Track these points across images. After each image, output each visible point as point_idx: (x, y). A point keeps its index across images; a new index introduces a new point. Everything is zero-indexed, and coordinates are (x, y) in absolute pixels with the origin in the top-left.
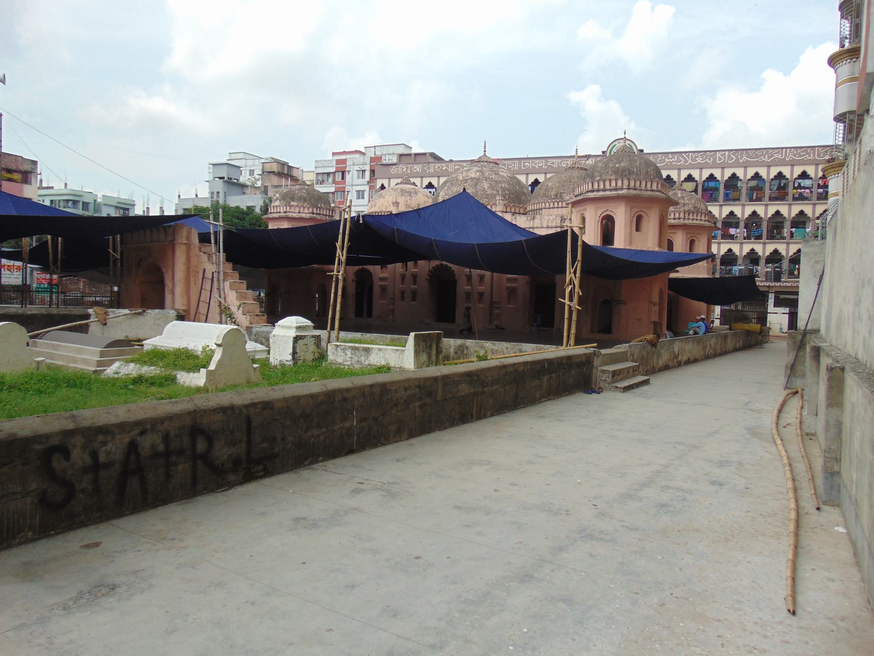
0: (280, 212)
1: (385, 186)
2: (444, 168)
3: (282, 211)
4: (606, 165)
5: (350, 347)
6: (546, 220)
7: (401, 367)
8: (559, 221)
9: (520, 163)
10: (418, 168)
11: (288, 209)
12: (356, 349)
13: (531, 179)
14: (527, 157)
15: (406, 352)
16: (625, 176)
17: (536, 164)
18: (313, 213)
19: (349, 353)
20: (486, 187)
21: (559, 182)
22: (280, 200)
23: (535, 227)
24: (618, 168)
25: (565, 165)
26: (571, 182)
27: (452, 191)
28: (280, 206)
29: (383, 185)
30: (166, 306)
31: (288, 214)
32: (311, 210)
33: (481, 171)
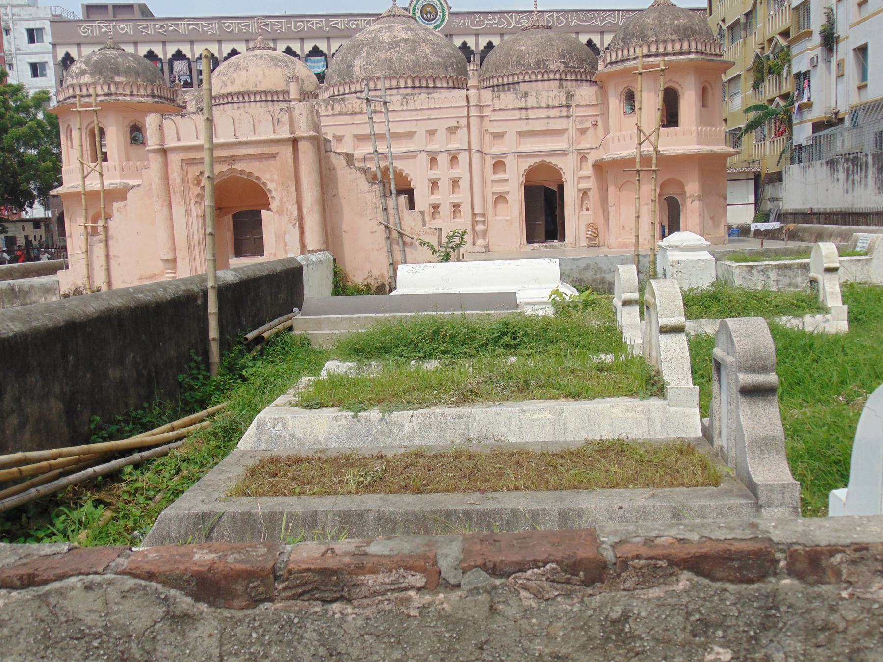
0: (125, 95)
2: (171, 29)
4: (660, 22)
5: (775, 266)
7: (866, 283)
8: (564, 98)
9: (289, 23)
10: (126, 28)
11: (113, 89)
13: (483, 42)
14: (284, 14)
15: (875, 261)
16: (689, 36)
17: (312, 24)
18: (153, 96)
19: (773, 275)
20: (428, 51)
22: (92, 75)
23: (529, 106)
24: (678, 25)
26: (552, 45)
27: (378, 58)
28: (94, 84)
29: (67, 55)
30: (682, 225)
31: (114, 97)
32: (149, 91)
33: (412, 30)
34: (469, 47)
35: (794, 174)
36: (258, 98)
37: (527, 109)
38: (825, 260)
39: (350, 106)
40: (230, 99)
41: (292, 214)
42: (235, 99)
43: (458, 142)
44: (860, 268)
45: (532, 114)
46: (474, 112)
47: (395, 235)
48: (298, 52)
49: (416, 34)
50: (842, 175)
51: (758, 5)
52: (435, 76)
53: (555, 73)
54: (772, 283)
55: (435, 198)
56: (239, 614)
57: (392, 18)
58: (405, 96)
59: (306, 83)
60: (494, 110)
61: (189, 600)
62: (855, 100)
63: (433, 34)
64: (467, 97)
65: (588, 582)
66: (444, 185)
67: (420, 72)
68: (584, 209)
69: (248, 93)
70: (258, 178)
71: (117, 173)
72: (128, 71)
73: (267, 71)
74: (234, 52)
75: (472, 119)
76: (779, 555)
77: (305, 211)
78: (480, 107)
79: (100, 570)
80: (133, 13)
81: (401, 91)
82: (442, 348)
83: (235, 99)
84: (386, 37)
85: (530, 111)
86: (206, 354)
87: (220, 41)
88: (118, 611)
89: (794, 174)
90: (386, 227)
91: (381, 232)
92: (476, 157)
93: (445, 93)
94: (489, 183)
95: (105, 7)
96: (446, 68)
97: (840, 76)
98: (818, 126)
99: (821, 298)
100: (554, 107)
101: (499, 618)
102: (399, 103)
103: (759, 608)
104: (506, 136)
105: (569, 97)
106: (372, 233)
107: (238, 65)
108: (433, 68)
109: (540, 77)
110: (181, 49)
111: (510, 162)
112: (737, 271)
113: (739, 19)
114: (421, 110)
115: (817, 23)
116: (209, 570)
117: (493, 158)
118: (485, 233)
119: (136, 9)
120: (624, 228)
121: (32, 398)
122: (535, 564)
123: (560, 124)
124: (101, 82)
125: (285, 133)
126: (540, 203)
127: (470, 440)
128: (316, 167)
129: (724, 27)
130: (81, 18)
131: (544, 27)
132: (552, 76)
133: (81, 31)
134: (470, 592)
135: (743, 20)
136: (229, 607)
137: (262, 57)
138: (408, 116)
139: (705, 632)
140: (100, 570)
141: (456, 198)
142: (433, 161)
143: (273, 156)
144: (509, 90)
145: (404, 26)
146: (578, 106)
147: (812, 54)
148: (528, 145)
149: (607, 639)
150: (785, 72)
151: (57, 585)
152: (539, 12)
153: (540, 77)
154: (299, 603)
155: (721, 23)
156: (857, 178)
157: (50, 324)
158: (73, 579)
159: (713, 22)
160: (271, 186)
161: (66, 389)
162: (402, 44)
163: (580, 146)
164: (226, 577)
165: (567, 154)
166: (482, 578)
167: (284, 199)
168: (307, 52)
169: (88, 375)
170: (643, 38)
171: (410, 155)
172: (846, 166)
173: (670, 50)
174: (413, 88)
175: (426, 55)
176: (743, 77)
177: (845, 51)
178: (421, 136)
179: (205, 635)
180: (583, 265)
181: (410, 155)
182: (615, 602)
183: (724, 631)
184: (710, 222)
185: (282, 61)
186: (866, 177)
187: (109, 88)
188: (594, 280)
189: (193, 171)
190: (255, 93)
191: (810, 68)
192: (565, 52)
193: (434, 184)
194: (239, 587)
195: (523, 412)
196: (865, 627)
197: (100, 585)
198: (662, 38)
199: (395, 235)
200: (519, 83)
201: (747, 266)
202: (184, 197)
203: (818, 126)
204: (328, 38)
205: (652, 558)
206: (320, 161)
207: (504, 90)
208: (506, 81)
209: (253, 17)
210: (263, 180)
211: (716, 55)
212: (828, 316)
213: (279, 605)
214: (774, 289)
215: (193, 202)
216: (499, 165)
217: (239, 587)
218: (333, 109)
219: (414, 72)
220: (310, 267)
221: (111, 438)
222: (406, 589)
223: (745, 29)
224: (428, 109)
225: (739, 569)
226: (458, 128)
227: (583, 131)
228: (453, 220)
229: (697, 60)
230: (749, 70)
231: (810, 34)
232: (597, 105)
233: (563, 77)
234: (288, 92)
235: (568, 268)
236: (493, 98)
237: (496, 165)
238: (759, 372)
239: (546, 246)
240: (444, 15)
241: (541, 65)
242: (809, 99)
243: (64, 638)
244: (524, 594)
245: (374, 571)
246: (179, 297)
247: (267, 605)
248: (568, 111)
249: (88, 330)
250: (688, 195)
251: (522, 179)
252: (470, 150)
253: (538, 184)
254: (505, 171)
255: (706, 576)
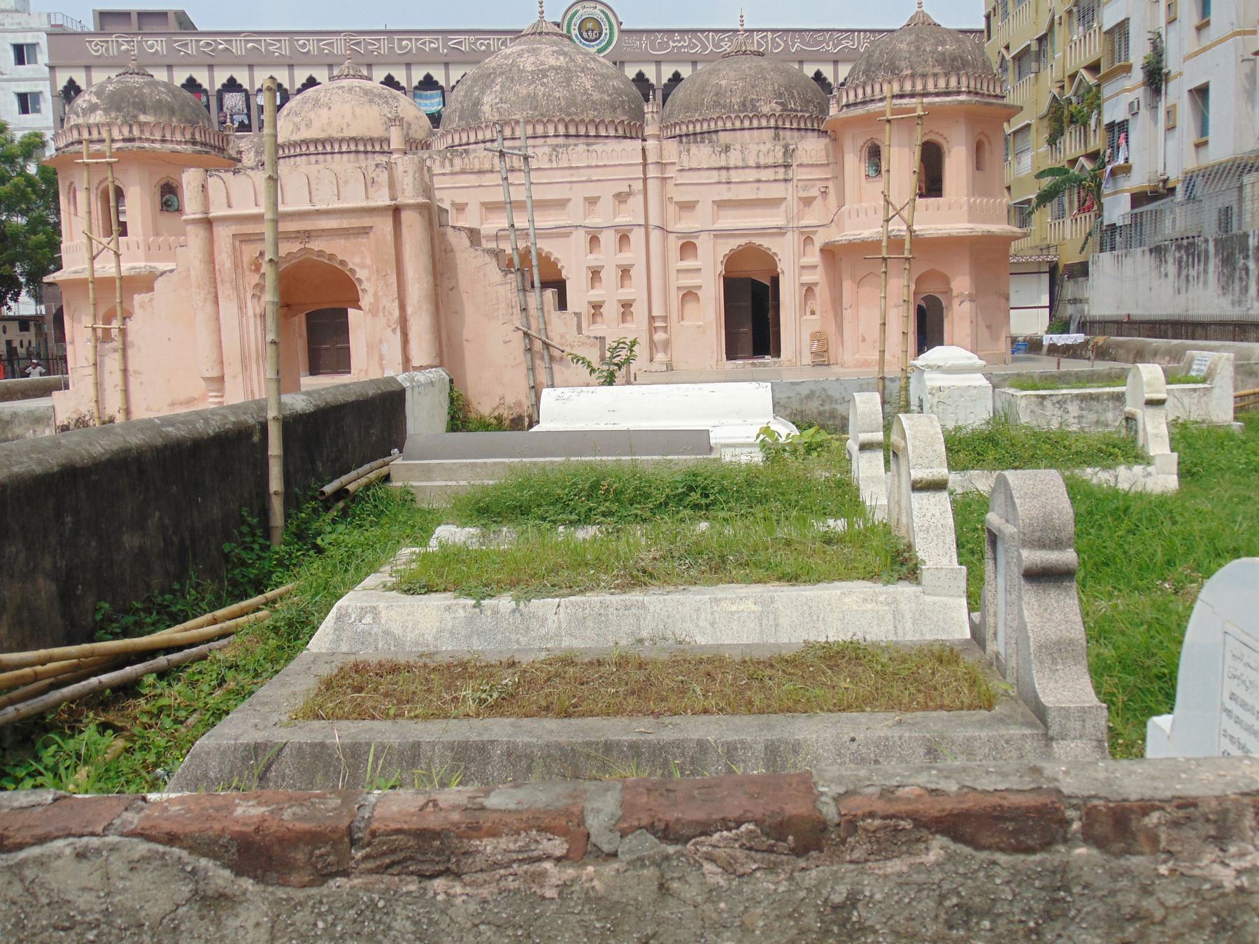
1: (78, 83)
2: (221, 47)
3: (116, 135)
4: (918, 48)
5: (1077, 395)
6: (755, 153)
7: (1203, 422)
8: (781, 154)
9: (391, 41)
10: (156, 45)
11: (136, 132)
12: (1092, 397)
13: (667, 72)
14: (382, 28)
15: (1217, 391)
16: (959, 69)
18: (194, 143)
19: (1073, 408)
20: (588, 85)
21: (744, 79)
22: (106, 111)
23: (732, 164)
25: (483, 48)
26: (765, 79)
27: (516, 94)
28: (109, 125)
29: (71, 82)
30: (946, 336)
31: (137, 144)
32: (188, 137)
33: (565, 54)
34: (647, 80)
35: (1104, 265)
36: (344, 148)
37: (728, 169)
38: (1145, 389)
39: (476, 161)
40: (304, 148)
41: (391, 314)
42: (312, 149)
43: (629, 215)
44: (1195, 401)
45: (735, 176)
46: (653, 172)
47: (538, 345)
48: (403, 83)
49: (572, 60)
50: (1172, 268)
51: (1056, 26)
52: (597, 120)
53: (768, 118)
54: (1072, 420)
55: (596, 294)
56: (300, 894)
57: (538, 37)
58: (555, 148)
59: (413, 126)
60: (682, 170)
61: (227, 873)
62: (1191, 162)
63: (595, 60)
64: (644, 150)
65: (801, 851)
66: (610, 275)
67: (576, 114)
68: (808, 312)
69: (331, 141)
70: (343, 263)
71: (141, 252)
72: (158, 107)
73: (358, 110)
74: (312, 82)
75: (649, 182)
76: (1070, 813)
77: (409, 310)
78: (662, 165)
79: (99, 829)
80: (167, 23)
81: (549, 141)
82: (603, 509)
83: (312, 149)
84: (528, 63)
85: (732, 172)
86: (264, 513)
87: (291, 66)
88: (125, 890)
89: (1104, 265)
90: (526, 334)
91: (518, 342)
92: (655, 235)
93: (612, 145)
94: (673, 274)
95: (125, 15)
96: (614, 109)
97: (1171, 128)
98: (1139, 199)
99: (1140, 442)
100: (766, 167)
101: (671, 902)
102: (546, 158)
103: (1042, 889)
104: (699, 207)
105: (787, 152)
106: (505, 342)
107: (317, 100)
108: (595, 109)
109: (747, 124)
110: (235, 76)
111: (703, 243)
112: (1023, 403)
113: (1029, 46)
114: (577, 168)
115: (1138, 53)
116: (257, 830)
117: (679, 238)
118: (667, 345)
119: (171, 18)
120: (864, 340)
121: (12, 576)
122: (725, 824)
123: (776, 191)
124: (119, 121)
125: (382, 199)
126: (746, 303)
127: (641, 641)
128: (426, 247)
129: (1008, 57)
130: (92, 29)
131: (753, 53)
132: (764, 123)
133: (91, 49)
134: (631, 863)
135: (1034, 48)
136: (285, 884)
137: (351, 89)
138: (558, 177)
139: (966, 923)
140: (99, 829)
141: (626, 294)
142: (594, 240)
143: (365, 231)
144: (702, 142)
145: (555, 48)
146: (800, 165)
147: (1130, 97)
148: (729, 221)
149: (827, 932)
150: (1093, 122)
151: (35, 851)
152: (746, 31)
153: (747, 124)
154: (386, 878)
155: (1003, 51)
156: (1193, 272)
157: (38, 470)
158: (60, 843)
159: (992, 49)
160: (361, 274)
161: (62, 564)
162: (551, 74)
163: (803, 223)
164: (281, 840)
165: (784, 234)
166: (648, 844)
167: (380, 294)
168: (415, 83)
169: (94, 544)
170: (893, 70)
171: (562, 233)
172: (1177, 255)
173: (931, 88)
174: (567, 136)
175: (586, 90)
176: (1033, 129)
177: (1177, 93)
178: (577, 206)
179: (250, 924)
180: (804, 391)
181: (562, 233)
182: (837, 879)
183: (993, 922)
184: (987, 333)
185: (380, 96)
186: (1206, 271)
187: (131, 131)
188: (820, 413)
189: (250, 251)
190: (341, 141)
191: (1128, 117)
192: (782, 89)
193: (595, 274)
194: (300, 856)
195: (718, 601)
196: (1191, 916)
197: (98, 851)
198: (920, 70)
199: (538, 345)
200: (717, 131)
201: (1037, 396)
202: (237, 289)
203: (1139, 199)
204: (446, 64)
205: (891, 817)
206: (432, 239)
207: (695, 142)
208: (698, 129)
209: (338, 33)
210: (351, 266)
211: (996, 96)
212: (1150, 469)
213: (357, 881)
214: (1074, 428)
215: (249, 295)
216: (688, 248)
217: (300, 856)
218: (452, 165)
219: (568, 114)
220: (416, 390)
221: (126, 633)
222: (539, 859)
223: (1038, 60)
224: (589, 167)
225: (1014, 833)
226: (629, 194)
227: (808, 202)
228: (622, 326)
229: (969, 102)
230: (1042, 118)
231: (1128, 69)
232: (828, 165)
233: (780, 124)
234: (388, 140)
235: (784, 395)
236: (680, 153)
237: (683, 247)
238: (1051, 548)
239: (753, 364)
240: (611, 33)
241: (750, 107)
242: (1127, 160)
243: (44, 928)
244: (708, 867)
245: (494, 833)
246: (226, 432)
247: (340, 881)
248: (786, 173)
249: (94, 478)
250: (955, 293)
251: (720, 268)
252: (646, 226)
253: (743, 275)
254: (696, 256)
255: (967, 842)
